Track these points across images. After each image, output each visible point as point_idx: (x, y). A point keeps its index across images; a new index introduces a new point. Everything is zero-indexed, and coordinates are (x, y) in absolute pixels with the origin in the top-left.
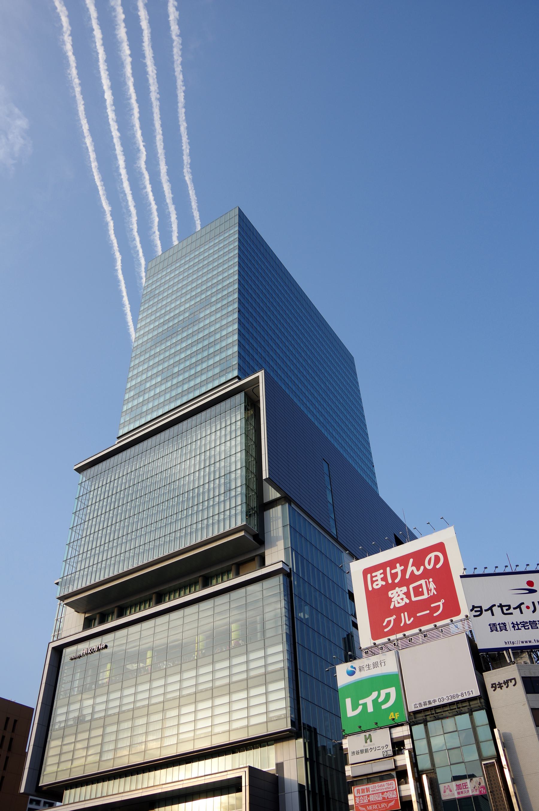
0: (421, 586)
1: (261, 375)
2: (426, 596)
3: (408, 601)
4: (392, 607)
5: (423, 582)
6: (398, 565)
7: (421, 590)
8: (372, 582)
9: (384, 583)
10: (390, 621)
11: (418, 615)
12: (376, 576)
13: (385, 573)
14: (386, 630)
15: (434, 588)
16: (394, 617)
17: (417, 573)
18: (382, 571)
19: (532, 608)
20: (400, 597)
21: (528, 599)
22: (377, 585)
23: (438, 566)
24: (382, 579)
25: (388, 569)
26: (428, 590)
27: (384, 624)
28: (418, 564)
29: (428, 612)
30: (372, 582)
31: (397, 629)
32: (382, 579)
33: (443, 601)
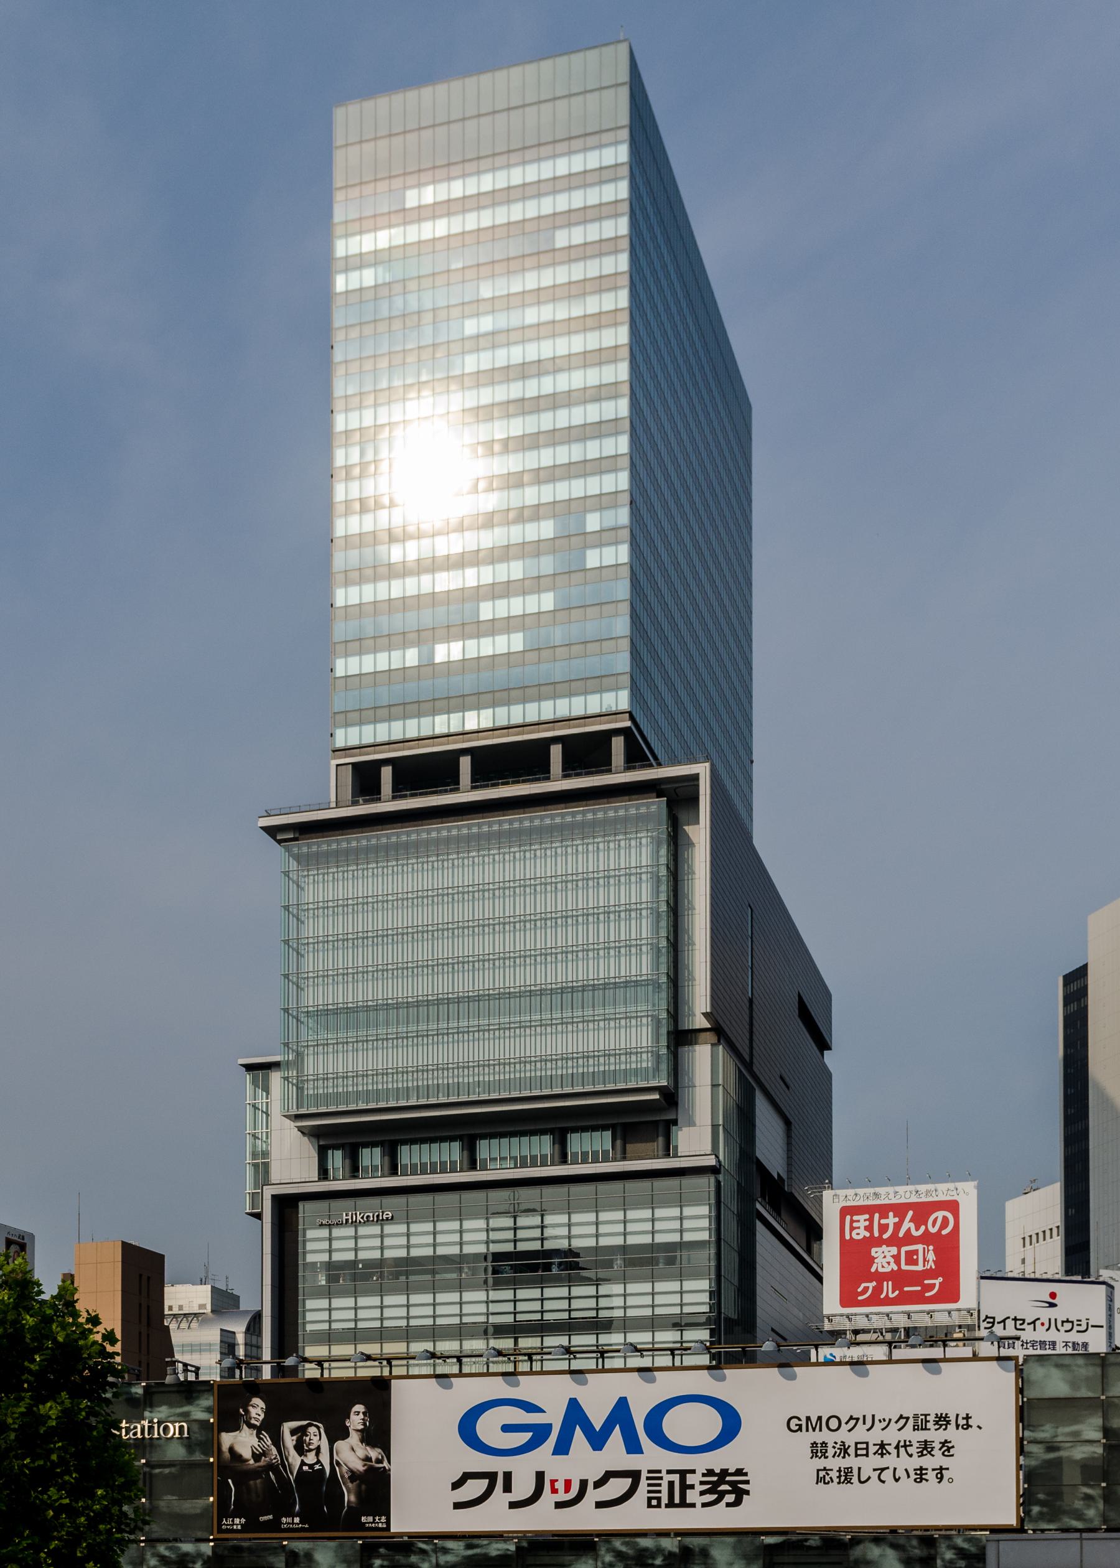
0: (916, 1252)
1: (702, 770)
2: (920, 1267)
3: (896, 1268)
4: (873, 1270)
5: (920, 1247)
6: (891, 1214)
8: (852, 1229)
9: (868, 1234)
10: (868, 1288)
11: (906, 1289)
13: (871, 1220)
14: (860, 1298)
16: (874, 1283)
17: (915, 1233)
18: (867, 1216)
19: (1047, 1326)
21: (1046, 1314)
23: (944, 1232)
24: (866, 1228)
25: (877, 1216)
27: (860, 1290)
28: (919, 1220)
29: (919, 1288)
30: (852, 1229)
31: (875, 1299)
32: (866, 1228)
33: (940, 1279)
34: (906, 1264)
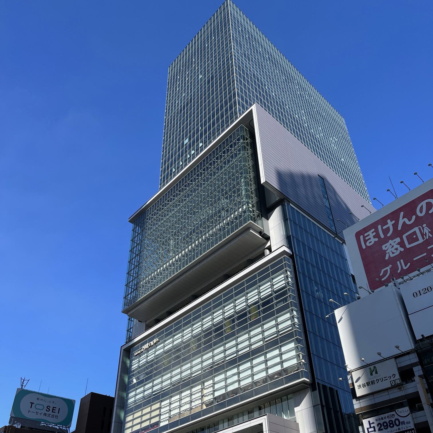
0: (415, 233)
2: (421, 241)
3: (402, 250)
4: (387, 258)
5: (416, 229)
6: (389, 221)
7: (415, 236)
8: (365, 241)
9: (377, 239)
10: (387, 270)
11: (415, 259)
12: (369, 235)
13: (377, 231)
15: (429, 232)
17: (408, 223)
18: (373, 230)
20: (395, 247)
22: (370, 242)
24: (374, 237)
26: (422, 235)
27: (381, 275)
31: (395, 275)
32: (374, 237)
34: (409, 244)
